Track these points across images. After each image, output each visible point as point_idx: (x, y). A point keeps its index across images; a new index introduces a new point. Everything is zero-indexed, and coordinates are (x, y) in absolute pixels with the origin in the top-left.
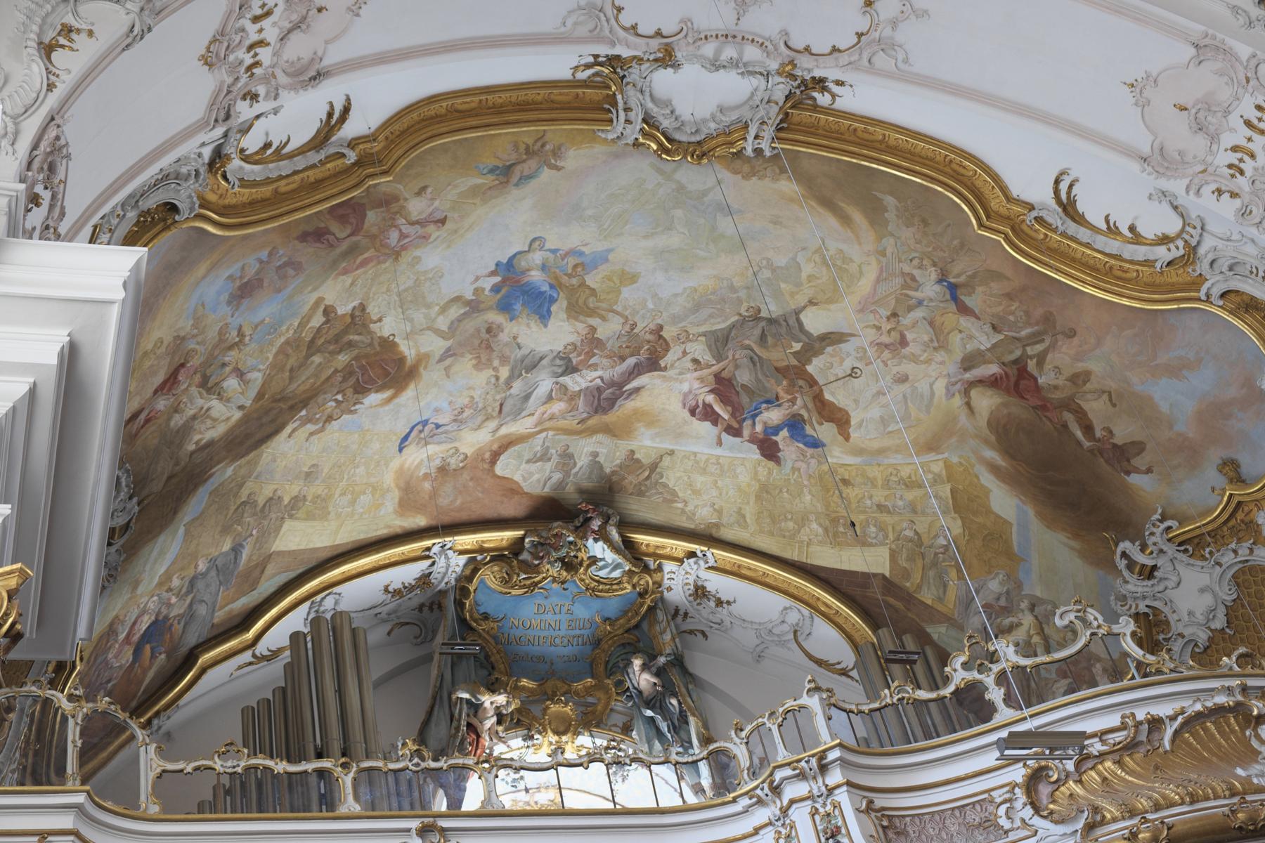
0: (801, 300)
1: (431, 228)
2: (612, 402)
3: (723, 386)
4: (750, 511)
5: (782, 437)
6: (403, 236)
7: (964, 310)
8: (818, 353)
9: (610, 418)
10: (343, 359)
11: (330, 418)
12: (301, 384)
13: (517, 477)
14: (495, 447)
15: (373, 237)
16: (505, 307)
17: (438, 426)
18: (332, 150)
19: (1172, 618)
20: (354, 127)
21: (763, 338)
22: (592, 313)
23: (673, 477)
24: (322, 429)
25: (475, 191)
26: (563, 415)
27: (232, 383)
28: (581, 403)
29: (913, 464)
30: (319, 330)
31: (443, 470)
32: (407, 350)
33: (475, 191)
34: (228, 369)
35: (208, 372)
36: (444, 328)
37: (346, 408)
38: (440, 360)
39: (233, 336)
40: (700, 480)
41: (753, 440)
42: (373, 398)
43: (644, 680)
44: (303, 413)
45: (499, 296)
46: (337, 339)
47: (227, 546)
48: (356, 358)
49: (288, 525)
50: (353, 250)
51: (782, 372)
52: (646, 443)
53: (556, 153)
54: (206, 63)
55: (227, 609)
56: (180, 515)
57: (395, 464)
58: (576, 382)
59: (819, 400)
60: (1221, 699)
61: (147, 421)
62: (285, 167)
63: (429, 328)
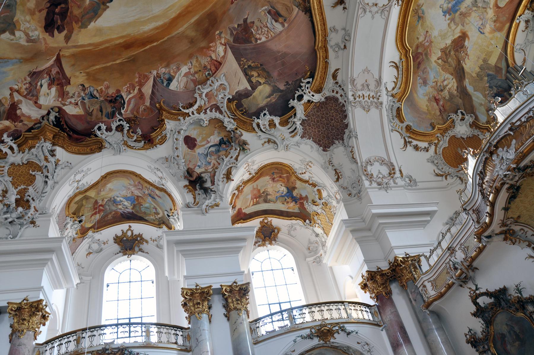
1: (428, 34)
10: (452, 53)
11: (466, 54)
12: (453, 63)
14: (495, 8)
15: (425, 49)
16: (456, 11)
17: (482, 24)
18: (401, 64)
20: (397, 60)
24: (468, 56)
25: (422, 25)
30: (442, 60)
33: (422, 25)
34: (442, 84)
35: (440, 90)
36: (455, 27)
38: (464, 26)
42: (466, 43)
44: (461, 62)
45: (452, 14)
46: (446, 55)
47: (486, 78)
48: (453, 49)
49: (489, 62)
50: (426, 55)
53: (418, 6)
54: (368, 111)
55: (503, 75)
56: (471, 94)
61: (443, 107)
62: (400, 76)
63: (454, 31)
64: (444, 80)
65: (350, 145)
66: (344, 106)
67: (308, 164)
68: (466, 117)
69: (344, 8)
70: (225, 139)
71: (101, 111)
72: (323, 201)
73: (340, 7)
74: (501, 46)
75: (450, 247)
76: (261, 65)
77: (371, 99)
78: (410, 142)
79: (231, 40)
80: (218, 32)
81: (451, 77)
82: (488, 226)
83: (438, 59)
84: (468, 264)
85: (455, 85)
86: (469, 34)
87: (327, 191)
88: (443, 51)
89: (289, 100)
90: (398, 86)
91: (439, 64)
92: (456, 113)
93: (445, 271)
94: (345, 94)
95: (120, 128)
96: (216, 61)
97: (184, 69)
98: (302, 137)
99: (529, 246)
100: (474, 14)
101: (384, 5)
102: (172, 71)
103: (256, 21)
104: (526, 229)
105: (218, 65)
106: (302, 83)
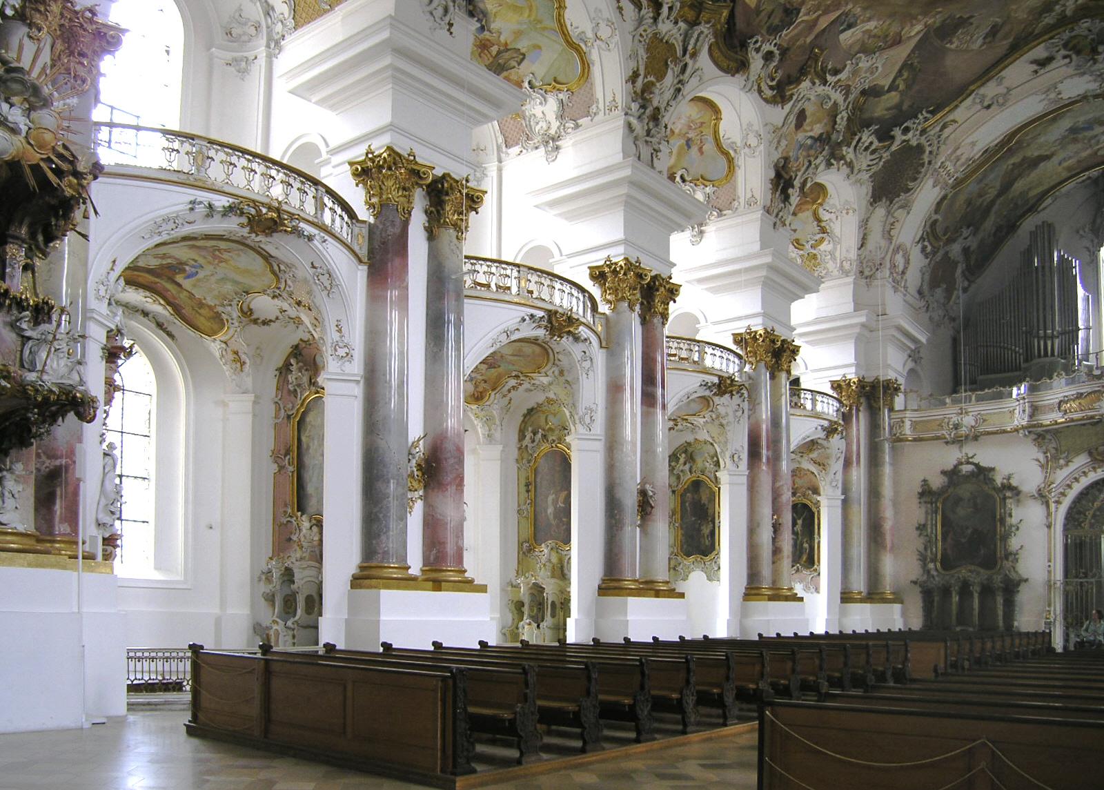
27: (990, 191)
32: (1048, 153)
42: (1042, 164)
47: (1012, 205)
64: (991, 187)
65: (895, 215)
66: (923, 167)
68: (970, 238)
69: (1036, 72)
70: (824, 136)
71: (769, 18)
73: (1035, 67)
74: (1052, 183)
76: (920, 70)
78: (924, 241)
79: (938, 24)
80: (940, 10)
87: (835, 249)
88: (1024, 159)
89: (896, 126)
92: (968, 227)
94: (937, 154)
95: (768, 56)
96: (901, 37)
97: (871, 25)
98: (871, 177)
100: (1079, 146)
102: (862, 18)
103: (974, 26)
105: (898, 41)
106: (922, 114)
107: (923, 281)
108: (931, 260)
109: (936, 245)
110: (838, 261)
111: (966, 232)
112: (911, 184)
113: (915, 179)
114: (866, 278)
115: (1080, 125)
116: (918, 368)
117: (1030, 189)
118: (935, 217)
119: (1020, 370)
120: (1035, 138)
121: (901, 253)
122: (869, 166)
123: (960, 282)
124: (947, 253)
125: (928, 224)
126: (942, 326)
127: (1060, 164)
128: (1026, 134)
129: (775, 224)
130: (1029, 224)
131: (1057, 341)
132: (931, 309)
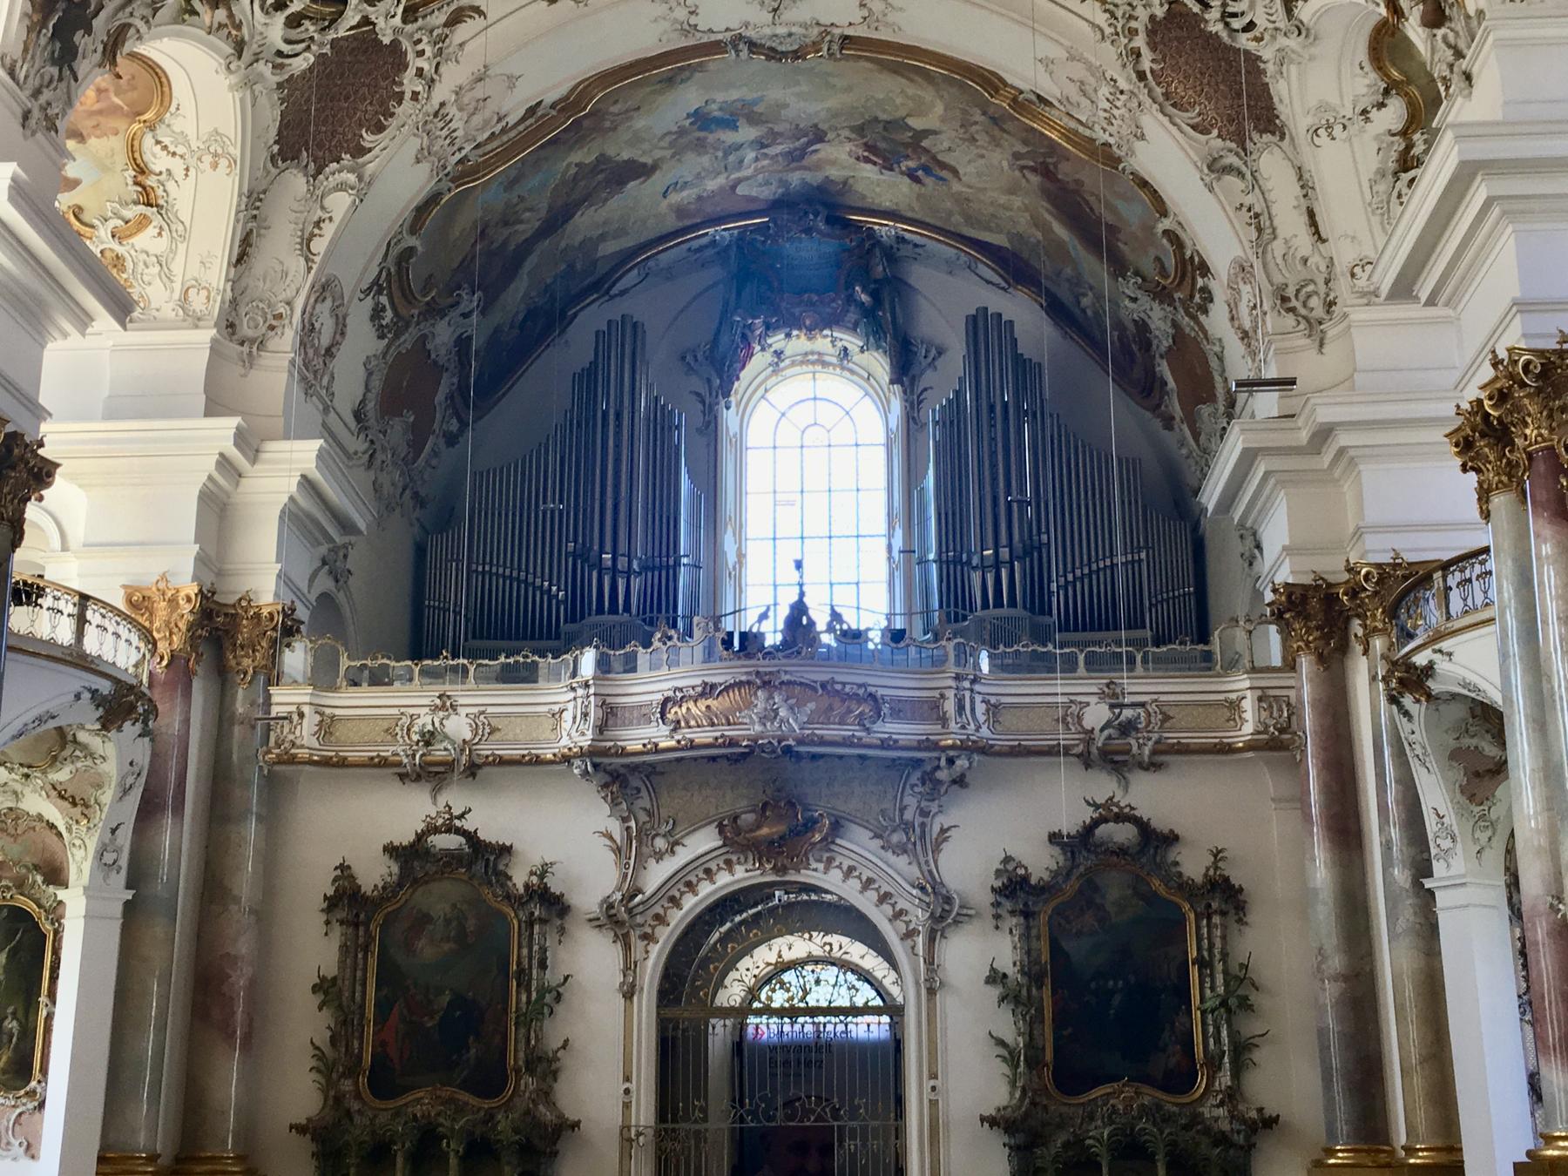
0: (902, 113)
2: (802, 157)
3: (868, 147)
4: (916, 206)
5: (920, 173)
6: (612, 122)
7: (1004, 130)
8: (926, 137)
9: (805, 162)
11: (606, 200)
13: (754, 194)
19: (1153, 327)
21: (885, 129)
22: (767, 122)
23: (860, 187)
25: (653, 92)
26: (769, 165)
28: (780, 158)
29: (1003, 199)
31: (700, 198)
37: (611, 195)
39: (515, 200)
40: (878, 190)
41: (902, 173)
42: (632, 184)
43: (864, 298)
47: (563, 267)
51: (906, 145)
52: (834, 173)
57: (665, 203)
58: (771, 151)
59: (934, 158)
60: (744, 678)
62: (512, 134)
64: (530, 210)
66: (400, 103)
67: (216, 155)
72: (120, 250)
75: (449, 697)
77: (448, 141)
78: (380, 292)
81: (543, 214)
82: (623, 753)
83: (576, 165)
84: (479, 761)
85: (528, 235)
86: (657, 175)
87: (174, 252)
88: (602, 159)
90: (489, 147)
91: (564, 175)
93: (386, 725)
98: (280, 86)
99: (624, 820)
100: (705, 160)
101: (696, 25)
104: (644, 793)
107: (367, 388)
108: (388, 346)
109: (403, 312)
110: (177, 286)
111: (470, 301)
112: (368, 138)
113: (380, 128)
114: (242, 344)
115: (714, 110)
116: (341, 597)
117: (603, 238)
118: (412, 241)
119: (558, 637)
120: (628, 114)
121: (328, 302)
122: (280, 53)
123: (444, 421)
124: (423, 339)
125: (394, 252)
126: (398, 510)
127: (665, 195)
128: (613, 98)
129: (26, 116)
130: (592, 318)
131: (636, 583)
132: (377, 462)
